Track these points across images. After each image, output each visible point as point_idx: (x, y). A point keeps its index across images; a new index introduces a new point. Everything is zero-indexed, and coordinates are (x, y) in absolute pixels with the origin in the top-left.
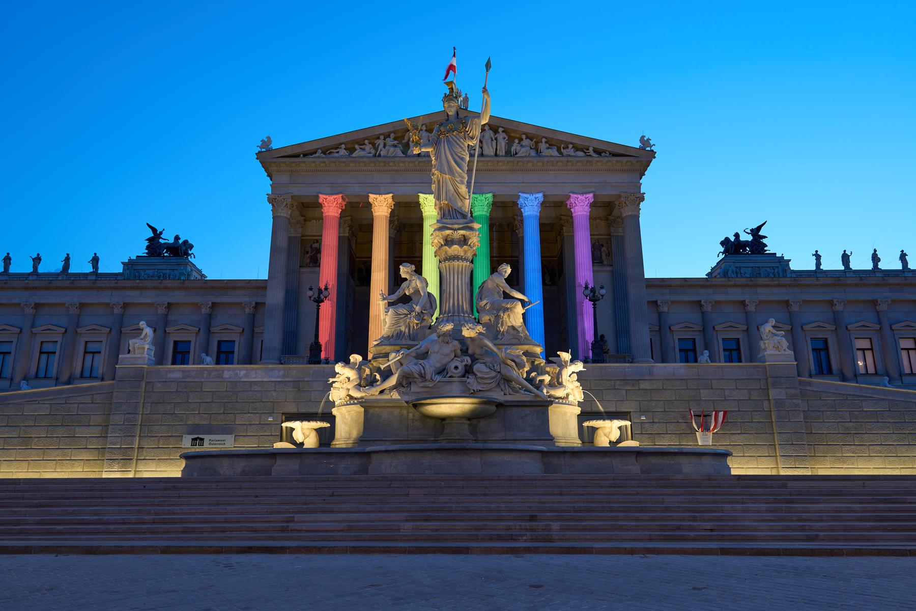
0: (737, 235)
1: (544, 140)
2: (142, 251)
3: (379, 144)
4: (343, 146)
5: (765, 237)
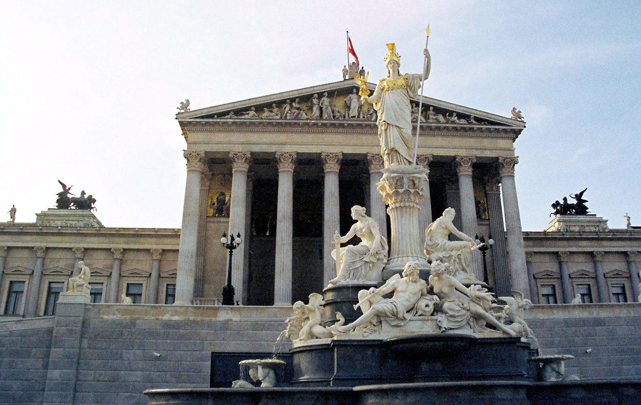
0: (565, 199)
1: (431, 108)
2: (54, 205)
3: (285, 108)
4: (252, 108)
5: (586, 201)
